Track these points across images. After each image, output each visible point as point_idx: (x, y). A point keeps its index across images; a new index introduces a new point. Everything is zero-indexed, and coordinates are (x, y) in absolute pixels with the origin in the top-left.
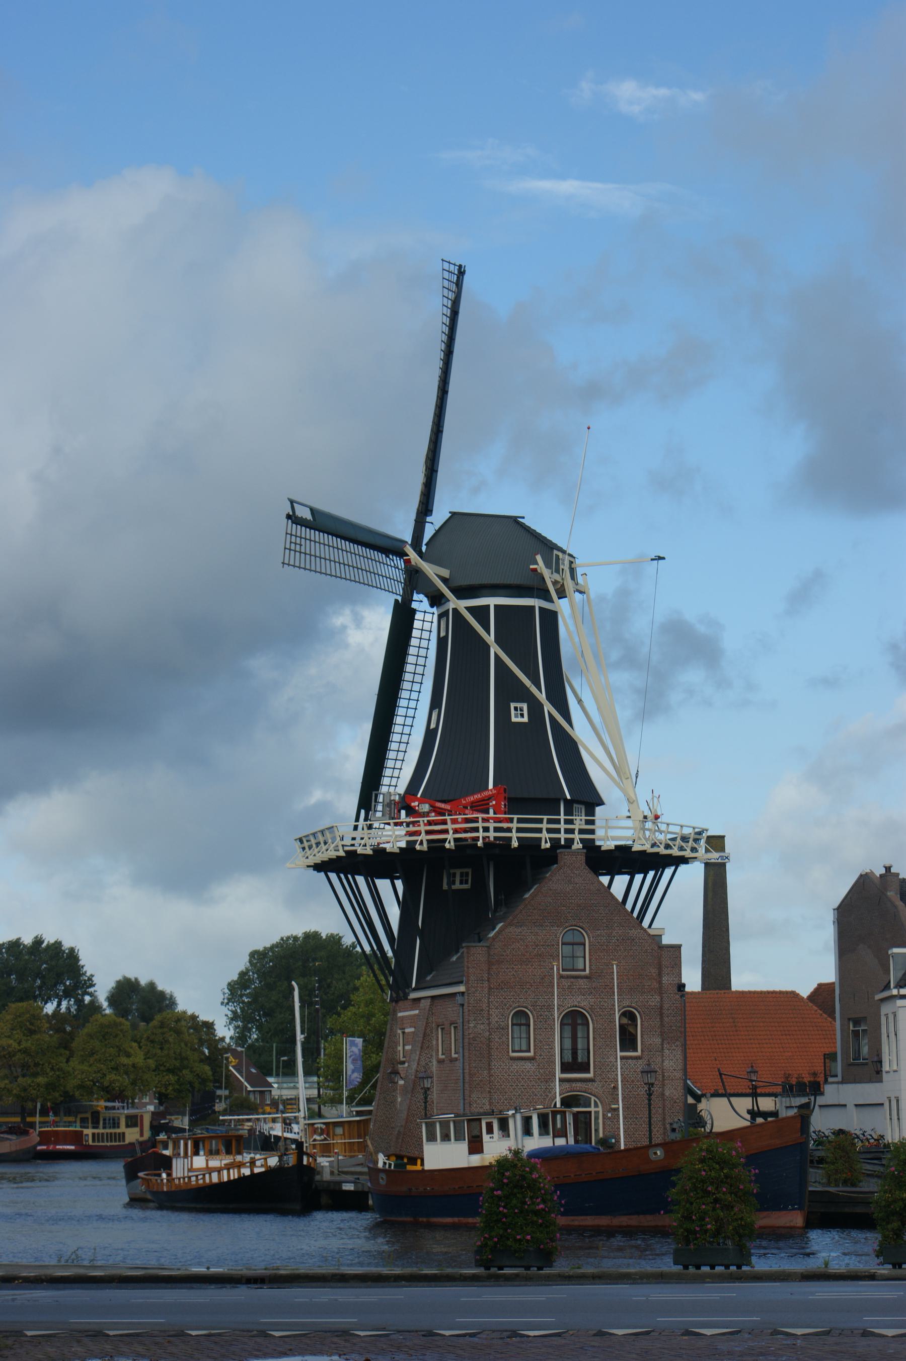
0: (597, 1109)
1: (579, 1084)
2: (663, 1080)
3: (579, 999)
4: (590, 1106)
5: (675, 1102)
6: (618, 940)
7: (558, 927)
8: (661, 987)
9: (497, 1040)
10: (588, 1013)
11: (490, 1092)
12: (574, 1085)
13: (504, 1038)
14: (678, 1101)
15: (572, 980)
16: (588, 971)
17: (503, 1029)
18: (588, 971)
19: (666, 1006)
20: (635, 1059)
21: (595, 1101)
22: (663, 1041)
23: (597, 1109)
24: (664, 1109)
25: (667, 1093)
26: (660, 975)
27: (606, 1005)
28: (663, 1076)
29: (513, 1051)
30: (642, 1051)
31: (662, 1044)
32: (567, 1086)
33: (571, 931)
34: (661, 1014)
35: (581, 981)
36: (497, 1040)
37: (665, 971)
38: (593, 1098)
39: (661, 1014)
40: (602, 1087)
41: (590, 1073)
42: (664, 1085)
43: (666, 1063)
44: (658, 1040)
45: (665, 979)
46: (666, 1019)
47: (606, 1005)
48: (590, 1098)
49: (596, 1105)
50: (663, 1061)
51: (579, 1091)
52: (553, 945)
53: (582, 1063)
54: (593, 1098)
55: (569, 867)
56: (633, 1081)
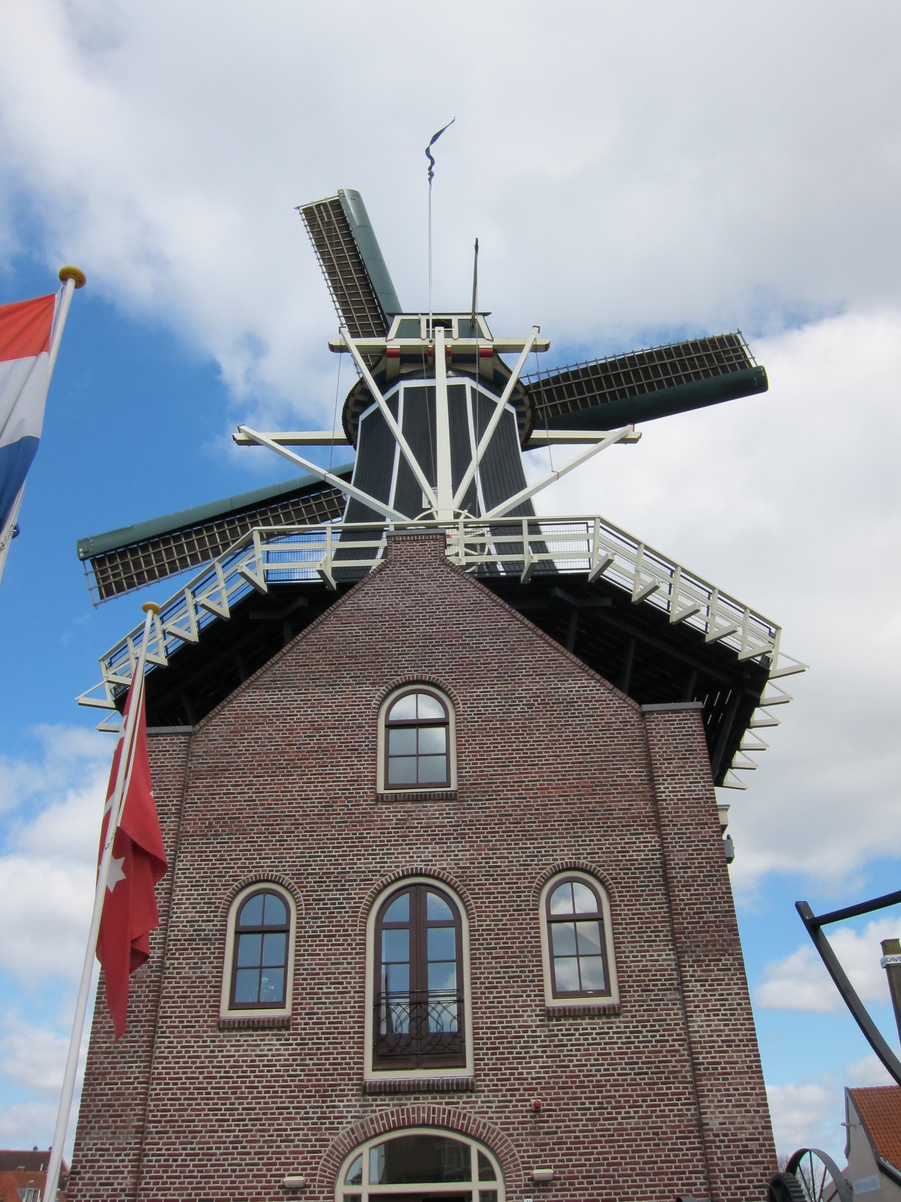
0: (488, 1185)
1: (426, 1102)
2: (696, 1077)
3: (427, 855)
4: (465, 1176)
5: (746, 1151)
6: (530, 706)
7: (373, 684)
8: (657, 814)
9: (186, 971)
10: (455, 889)
11: (141, 1130)
12: (410, 1103)
13: (207, 968)
14: (753, 1146)
15: (409, 805)
16: (454, 786)
17: (206, 940)
18: (454, 786)
19: (677, 858)
20: (599, 1016)
21: (480, 1154)
22: (680, 955)
23: (488, 1185)
24: (710, 1180)
25: (714, 1121)
26: (652, 780)
27: (504, 864)
28: (695, 1066)
29: (233, 1006)
30: (621, 990)
31: (679, 967)
32: (389, 1110)
33: (413, 697)
34: (667, 881)
35: (432, 807)
36: (186, 971)
37: (663, 768)
38: (475, 1147)
39: (667, 881)
40: (501, 1109)
41: (465, 1067)
42: (697, 1094)
43: (698, 1022)
44: (665, 957)
45: (665, 789)
46: (682, 894)
47: (504, 864)
48: (467, 1149)
49: (487, 1174)
50: (687, 1017)
51: (424, 1125)
52: (360, 726)
53: (440, 1035)
54: (475, 1147)
55: (405, 563)
56: (599, 1086)
